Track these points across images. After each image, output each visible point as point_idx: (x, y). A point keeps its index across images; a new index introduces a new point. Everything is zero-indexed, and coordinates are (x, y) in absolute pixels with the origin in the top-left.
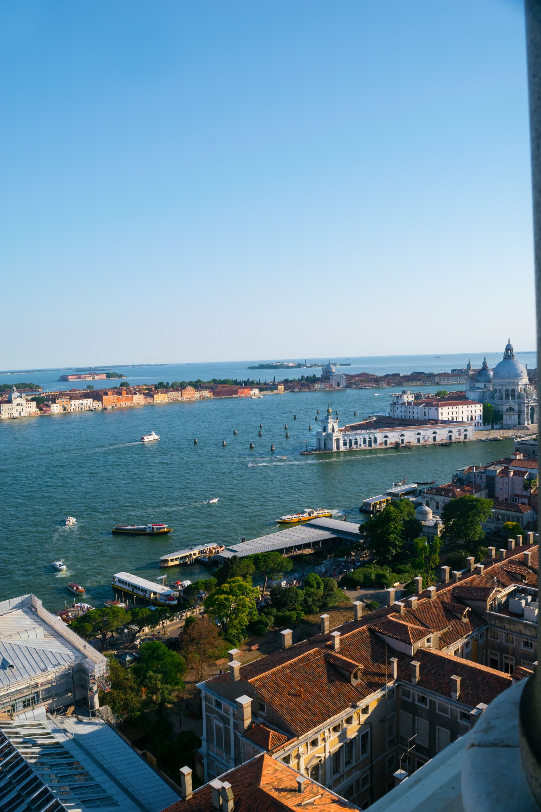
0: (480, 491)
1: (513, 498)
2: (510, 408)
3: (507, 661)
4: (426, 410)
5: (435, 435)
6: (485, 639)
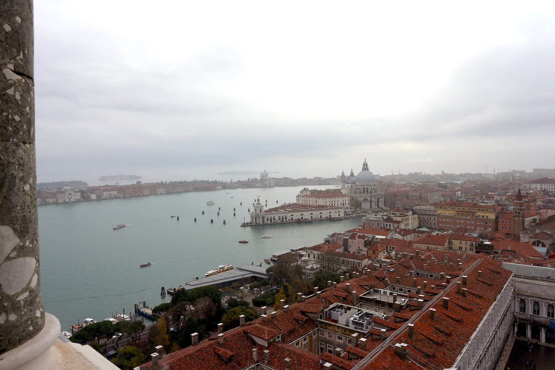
0: (339, 248)
2: (366, 199)
3: (330, 349)
5: (321, 215)
6: (317, 335)
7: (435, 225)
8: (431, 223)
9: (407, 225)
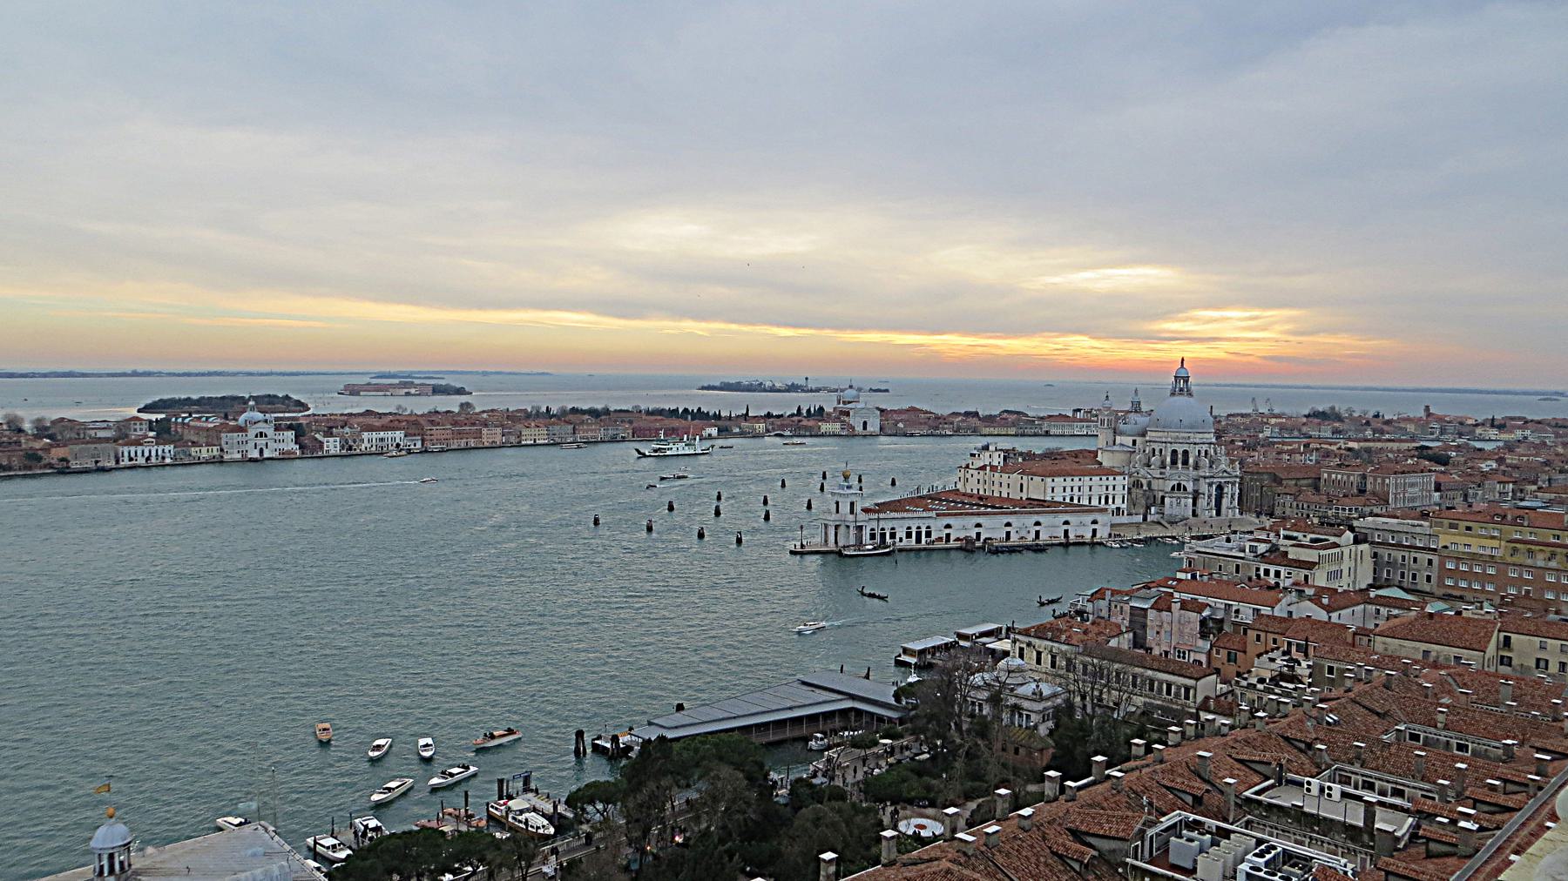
0: (1118, 635)
1: (1179, 652)
2: (1179, 485)
5: (1037, 528)
7: (1429, 579)
8: (1414, 576)
9: (1336, 575)
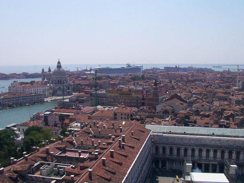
4: (24, 89)
